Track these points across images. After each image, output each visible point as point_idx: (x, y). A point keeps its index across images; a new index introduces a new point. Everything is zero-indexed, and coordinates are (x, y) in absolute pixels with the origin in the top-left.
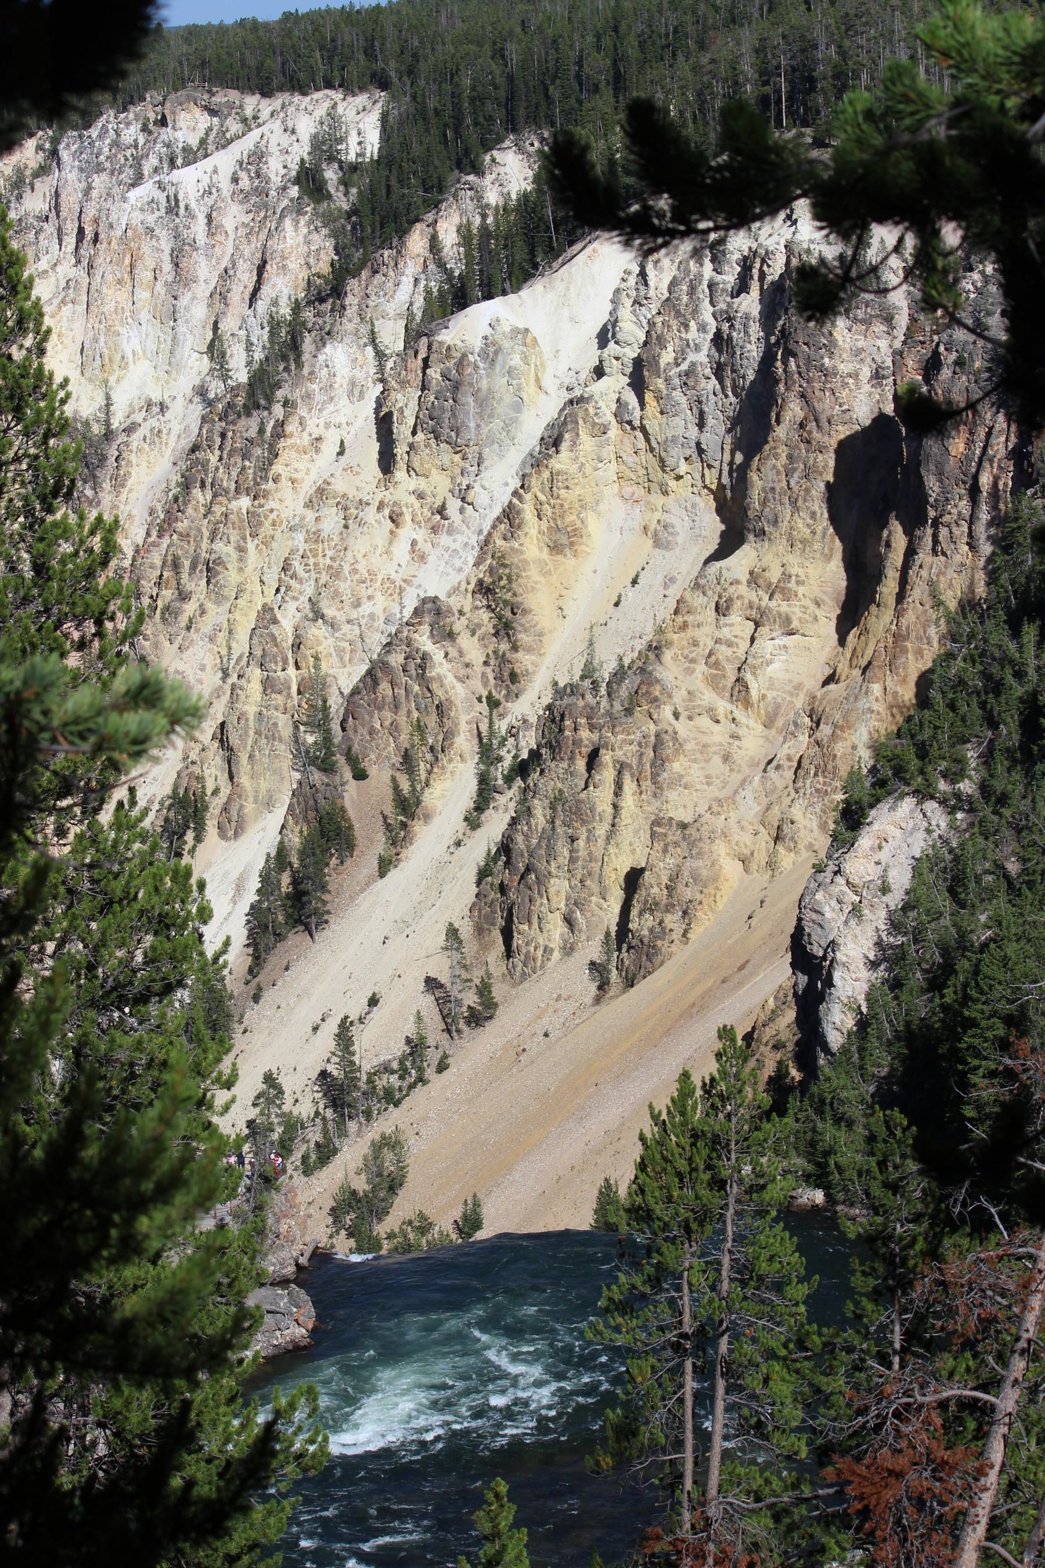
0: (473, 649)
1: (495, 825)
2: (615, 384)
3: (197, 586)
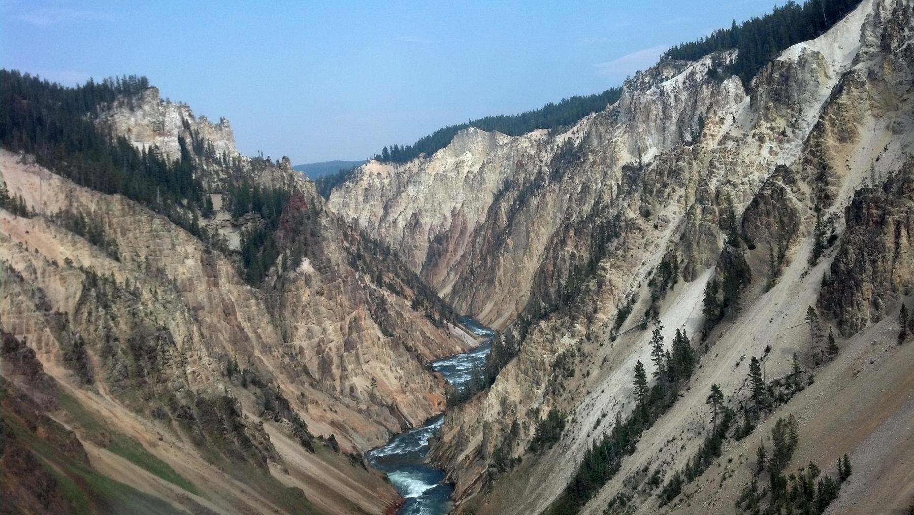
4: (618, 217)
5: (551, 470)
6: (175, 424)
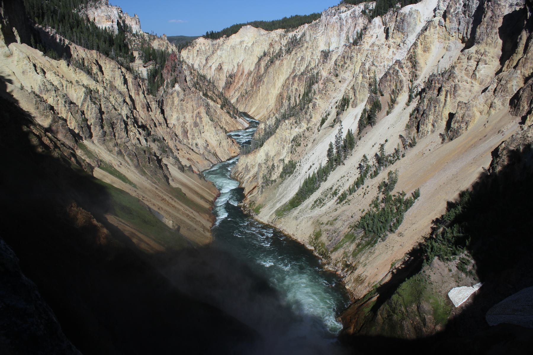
0: (407, 71)
1: (414, 105)
2: (439, 18)
3: (348, 62)
4: (317, 73)
5: (289, 185)
6: (126, 157)
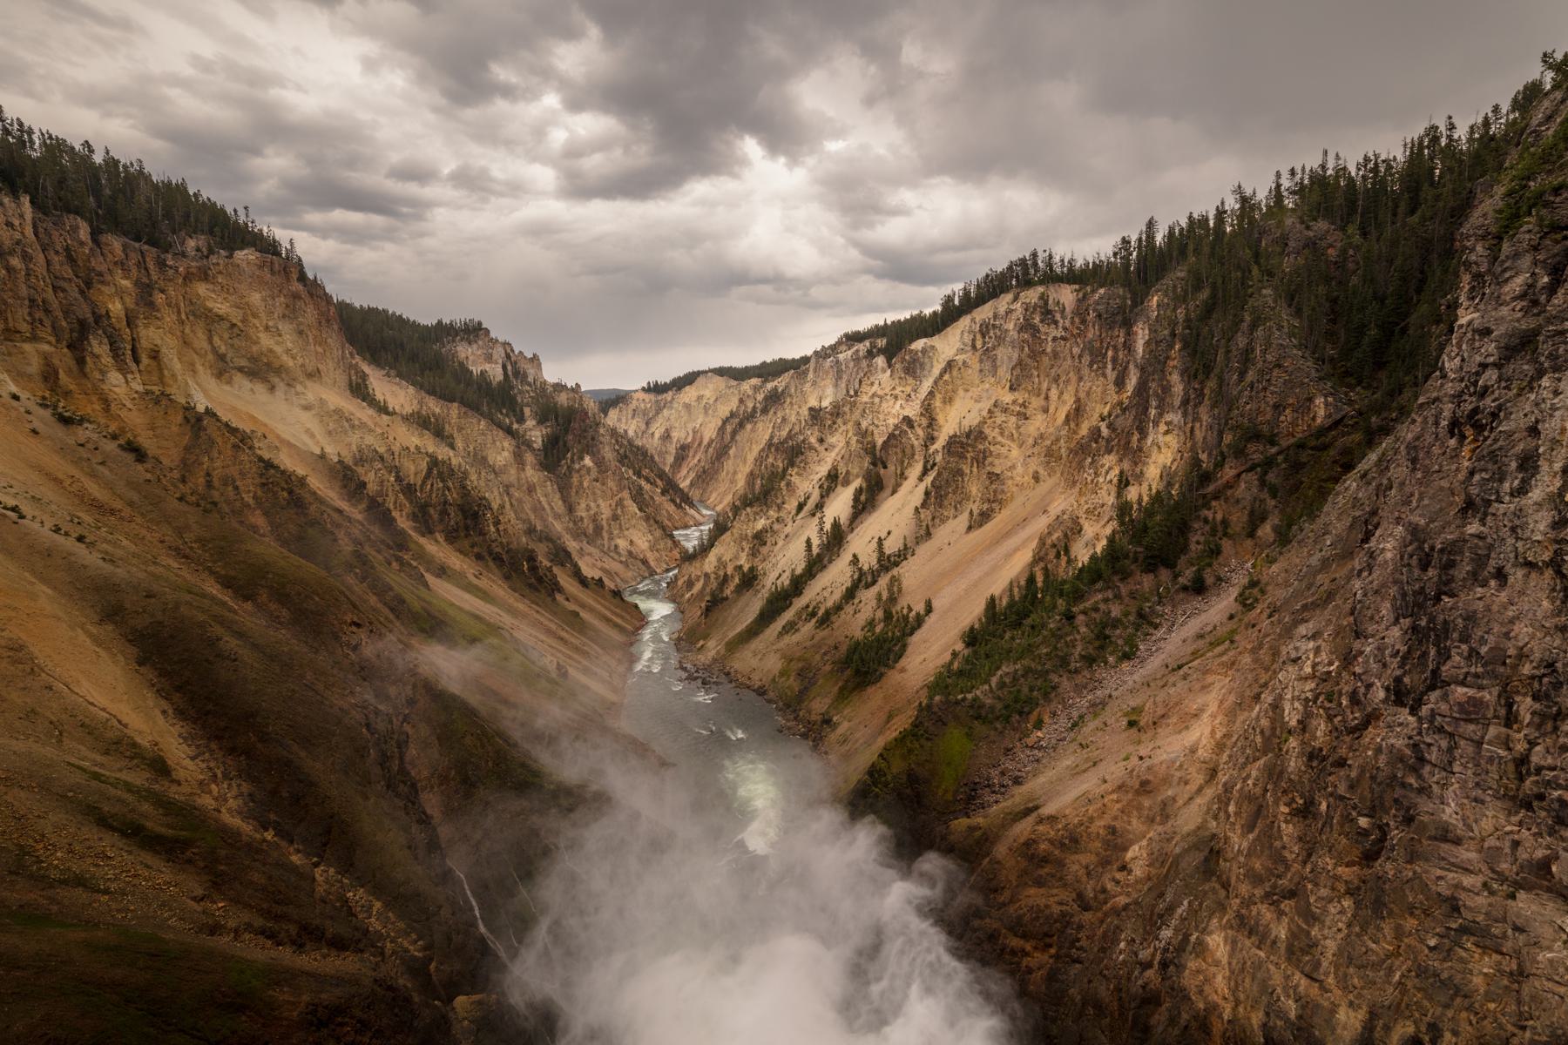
1: (929, 479)
